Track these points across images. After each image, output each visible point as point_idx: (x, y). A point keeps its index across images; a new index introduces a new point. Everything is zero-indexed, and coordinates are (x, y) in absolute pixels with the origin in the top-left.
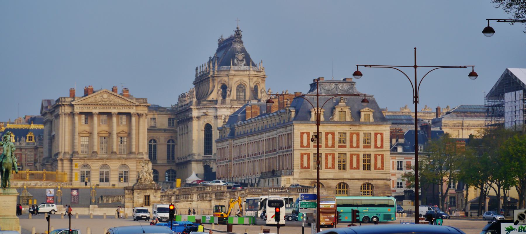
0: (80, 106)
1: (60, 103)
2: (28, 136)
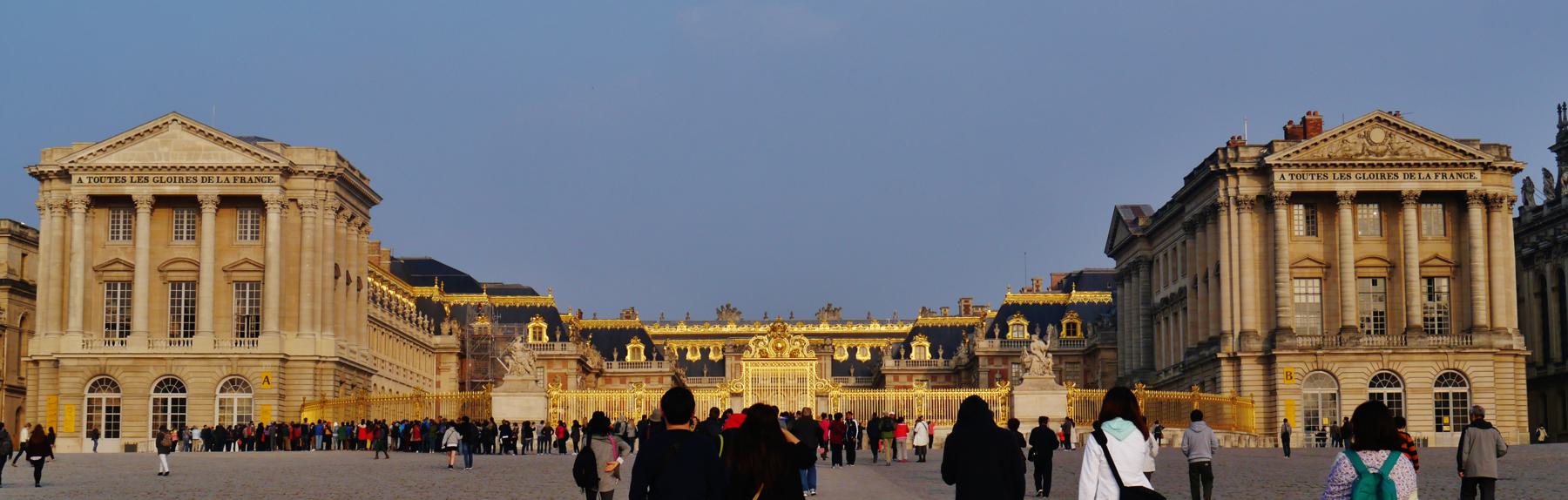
0: (1294, 170)
1: (1222, 166)
2: (1064, 322)
